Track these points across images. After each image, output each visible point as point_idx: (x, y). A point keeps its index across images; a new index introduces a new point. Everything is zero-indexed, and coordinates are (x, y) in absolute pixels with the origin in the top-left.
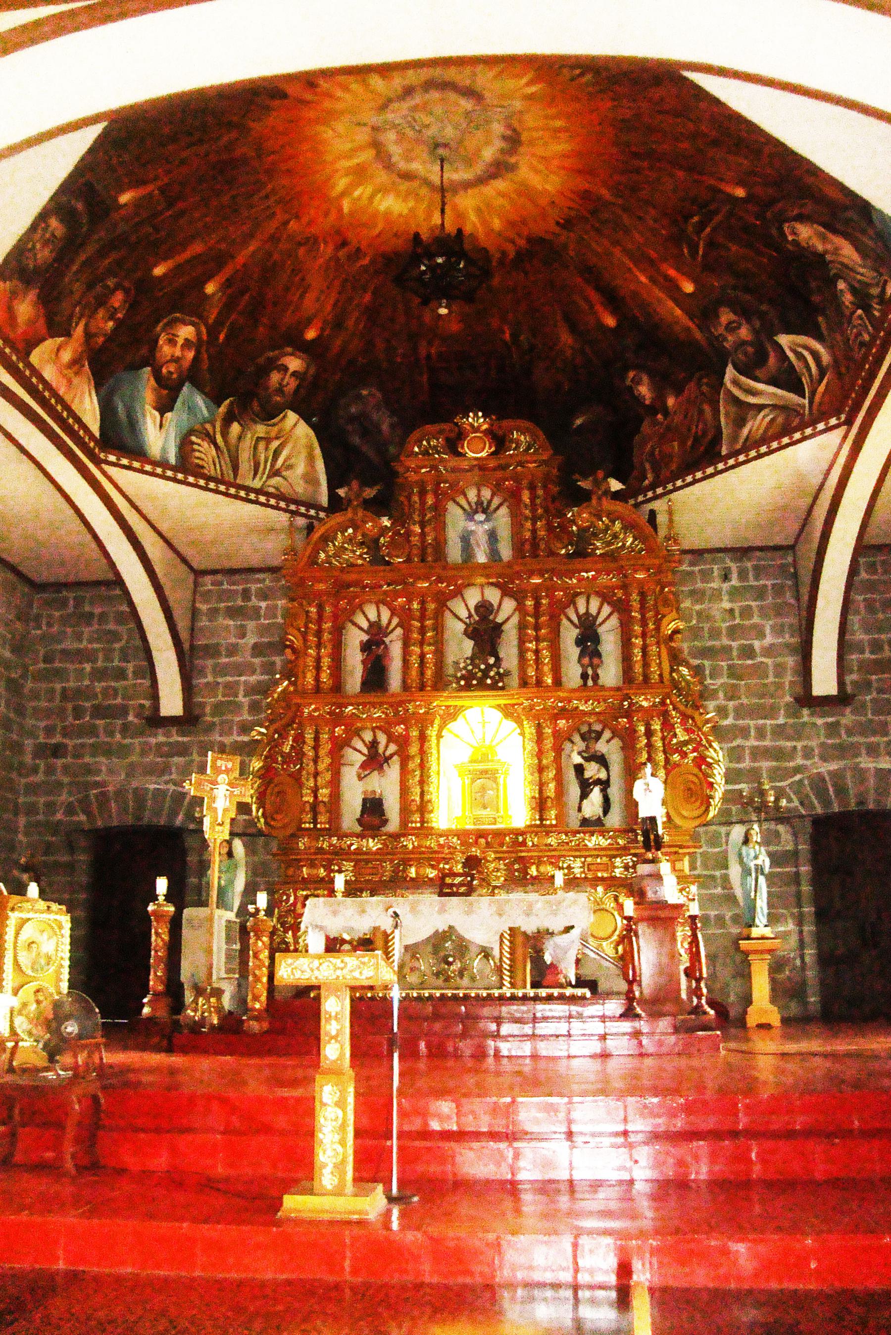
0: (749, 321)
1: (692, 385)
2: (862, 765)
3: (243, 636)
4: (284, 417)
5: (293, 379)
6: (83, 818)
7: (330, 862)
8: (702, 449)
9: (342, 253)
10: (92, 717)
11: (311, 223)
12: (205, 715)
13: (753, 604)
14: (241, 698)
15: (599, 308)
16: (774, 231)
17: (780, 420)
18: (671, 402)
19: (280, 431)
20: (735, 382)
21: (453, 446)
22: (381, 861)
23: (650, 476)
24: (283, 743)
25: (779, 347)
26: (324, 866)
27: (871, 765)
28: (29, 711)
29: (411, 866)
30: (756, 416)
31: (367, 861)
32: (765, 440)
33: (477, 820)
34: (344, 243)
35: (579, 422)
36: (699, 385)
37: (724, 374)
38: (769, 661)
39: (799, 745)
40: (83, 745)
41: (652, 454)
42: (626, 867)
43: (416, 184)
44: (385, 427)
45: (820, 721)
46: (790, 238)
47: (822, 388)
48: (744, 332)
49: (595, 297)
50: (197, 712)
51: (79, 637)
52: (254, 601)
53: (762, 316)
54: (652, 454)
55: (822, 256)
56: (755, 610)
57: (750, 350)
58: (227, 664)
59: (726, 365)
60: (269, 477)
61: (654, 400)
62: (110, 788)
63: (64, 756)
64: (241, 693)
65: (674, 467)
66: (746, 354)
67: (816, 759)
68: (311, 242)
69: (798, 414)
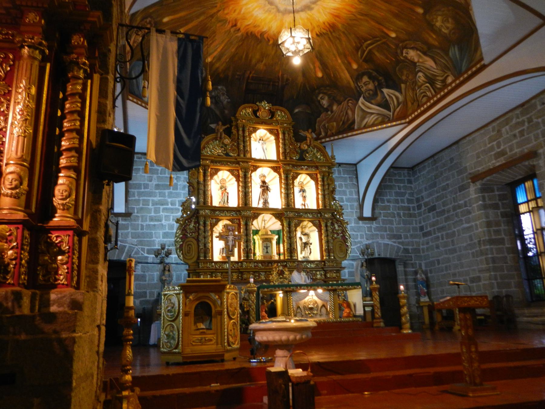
0: (373, 82)
1: (346, 102)
2: (380, 242)
3: (151, 181)
7: (212, 273)
8: (346, 126)
9: (232, 30)
11: (227, 14)
12: (135, 213)
13: (343, 183)
14: (150, 206)
15: (317, 69)
16: (399, 51)
17: (380, 119)
18: (335, 108)
20: (363, 104)
21: (255, 112)
23: (323, 134)
24: (190, 225)
25: (382, 92)
26: (210, 275)
27: (382, 242)
29: (244, 274)
30: (371, 116)
32: (373, 125)
34: (236, 25)
35: (296, 110)
36: (348, 103)
37: (359, 100)
38: (349, 204)
39: (359, 234)
41: (324, 125)
42: (321, 275)
43: (273, 7)
45: (365, 226)
46: (404, 55)
47: (398, 109)
48: (371, 86)
49: (318, 64)
50: (130, 211)
52: (156, 167)
53: (379, 81)
54: (324, 125)
55: (415, 63)
56: (344, 185)
57: (371, 92)
58: (143, 192)
59: (360, 97)
64: (151, 204)
65: (334, 131)
66: (369, 94)
67: (365, 239)
68: (224, 21)
69: (388, 117)
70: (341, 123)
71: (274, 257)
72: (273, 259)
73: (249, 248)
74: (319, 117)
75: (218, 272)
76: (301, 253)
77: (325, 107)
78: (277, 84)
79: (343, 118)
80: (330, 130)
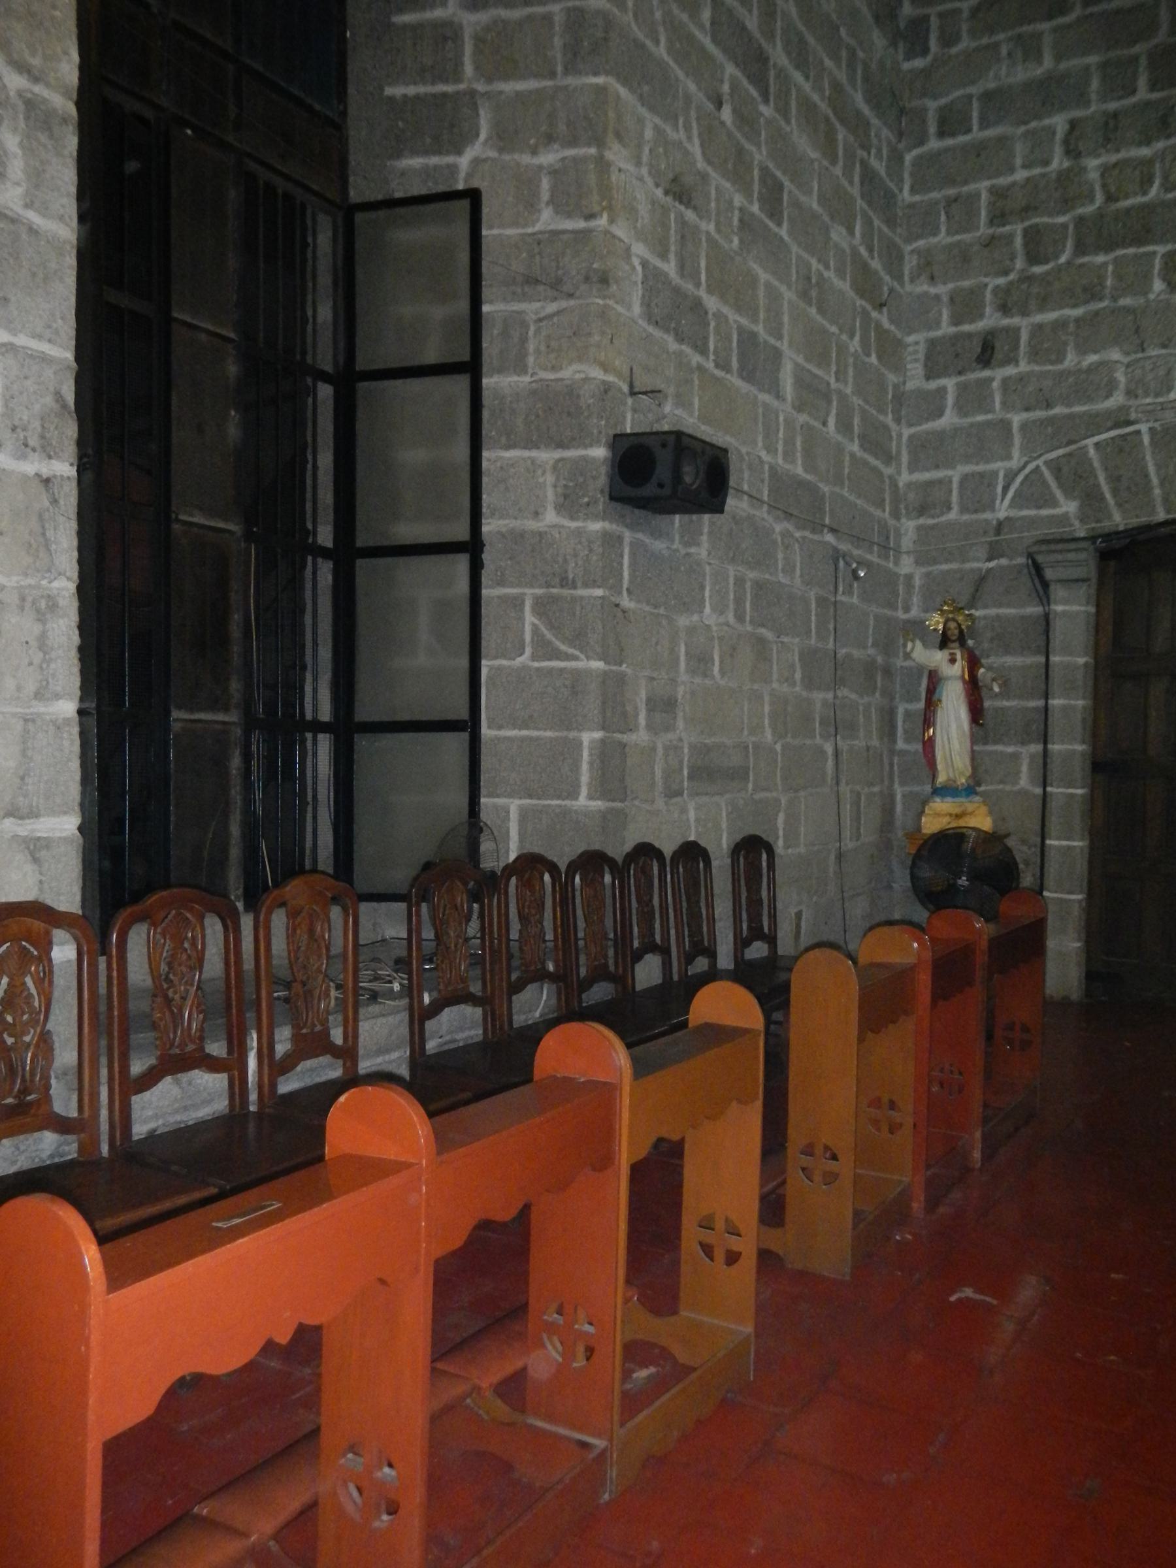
6: (1069, 507)
10: (1081, 248)
28: (910, 264)
40: (1060, 325)
51: (1030, 49)
62: (1143, 428)
63: (1012, 360)
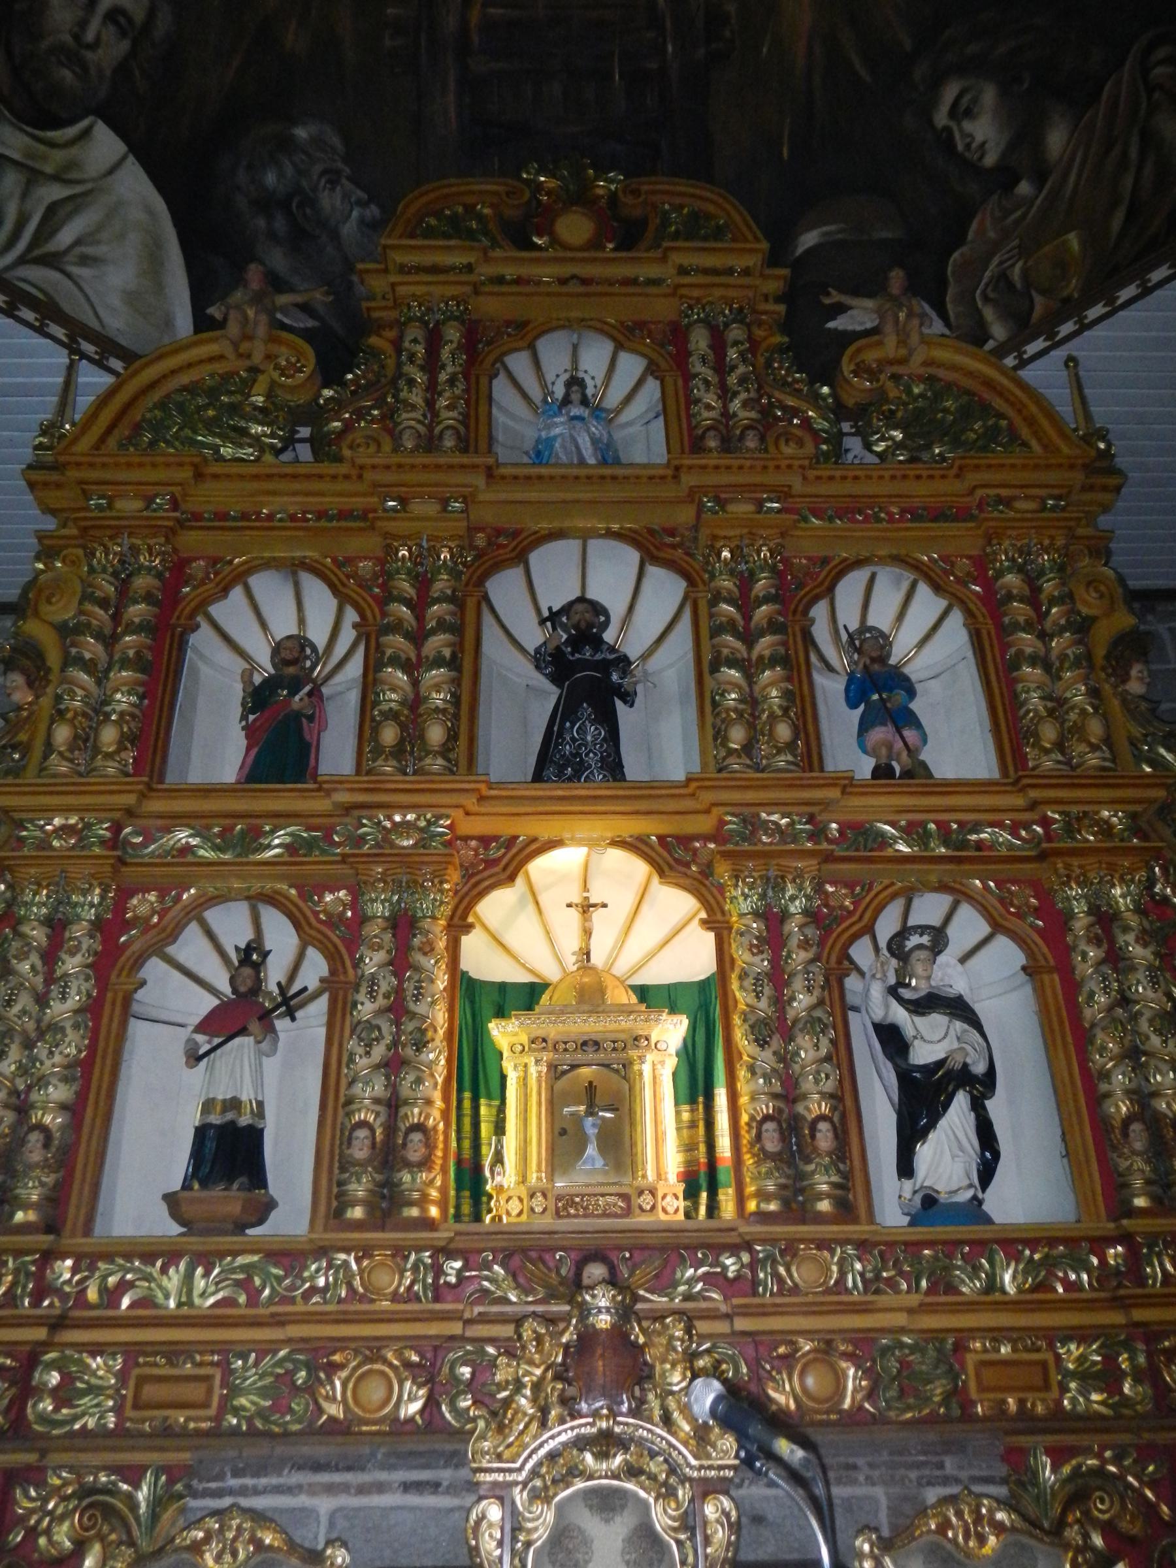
4: (86, 133)
5: (112, 28)
18: (1056, 140)
19: (72, 165)
22: (226, 1350)
29: (333, 1368)
31: (174, 1352)
33: (565, 1204)
35: (809, 239)
41: (1003, 277)
44: (349, 229)
54: (1003, 277)
60: (22, 261)
61: (1012, 147)
65: (1073, 287)
70: (1117, 222)
71: (646, 1201)
72: (641, 1220)
73: (415, 1114)
74: (959, 240)
75: (96, 1349)
76: (906, 1168)
77: (990, 160)
78: (654, 66)
79: (1128, 181)
80: (1043, 292)
